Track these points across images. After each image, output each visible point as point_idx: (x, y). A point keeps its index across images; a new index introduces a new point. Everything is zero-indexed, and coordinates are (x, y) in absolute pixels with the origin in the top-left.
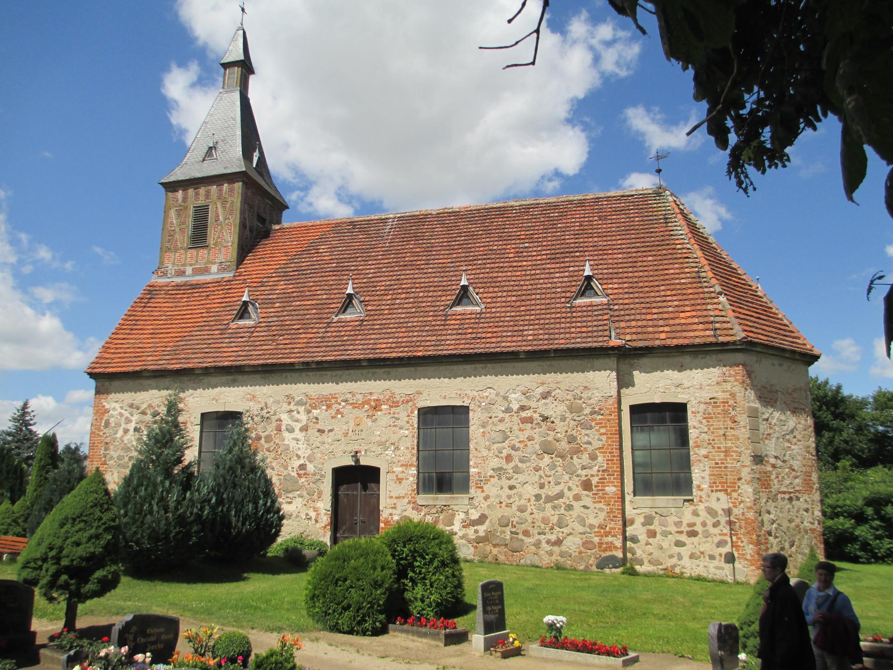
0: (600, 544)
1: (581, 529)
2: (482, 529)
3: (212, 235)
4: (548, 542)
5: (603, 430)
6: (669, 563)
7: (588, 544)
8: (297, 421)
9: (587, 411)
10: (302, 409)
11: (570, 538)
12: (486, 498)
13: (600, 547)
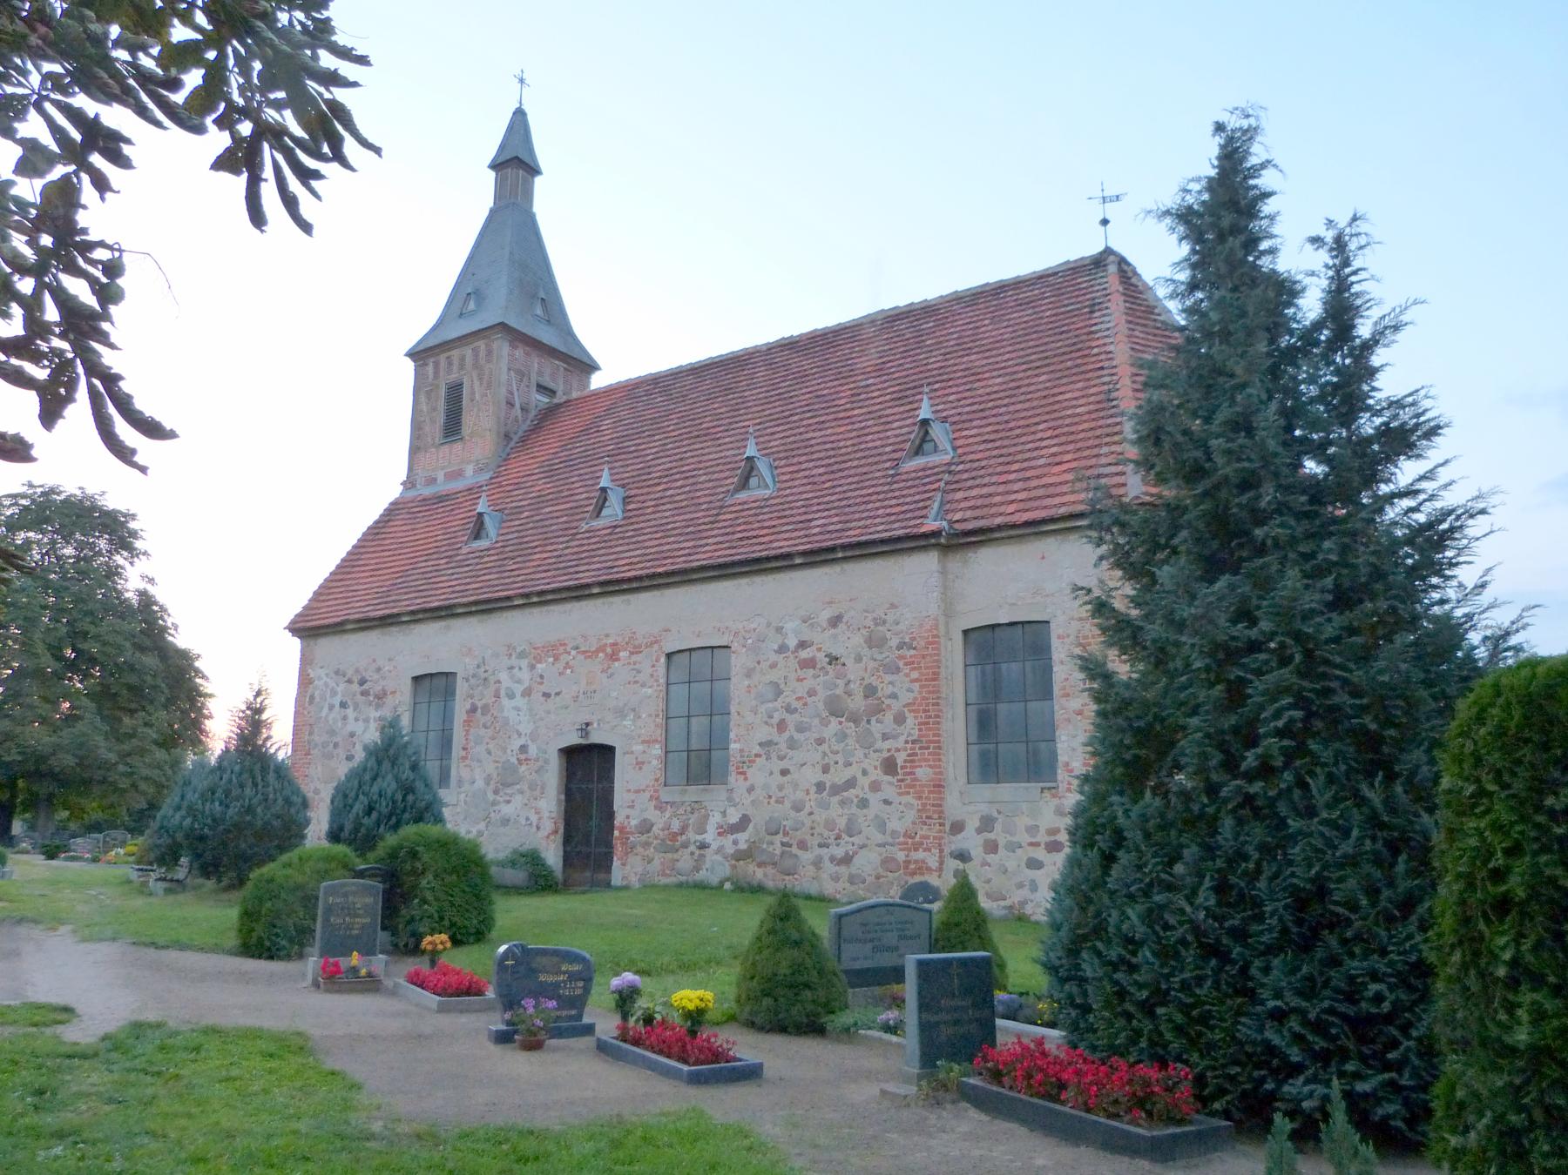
0: (907, 862)
1: (880, 838)
2: (743, 838)
3: (468, 421)
4: (832, 859)
5: (915, 675)
6: (1016, 897)
7: (888, 863)
8: (519, 682)
9: (894, 642)
10: (524, 663)
11: (863, 852)
12: (751, 790)
13: (906, 868)
